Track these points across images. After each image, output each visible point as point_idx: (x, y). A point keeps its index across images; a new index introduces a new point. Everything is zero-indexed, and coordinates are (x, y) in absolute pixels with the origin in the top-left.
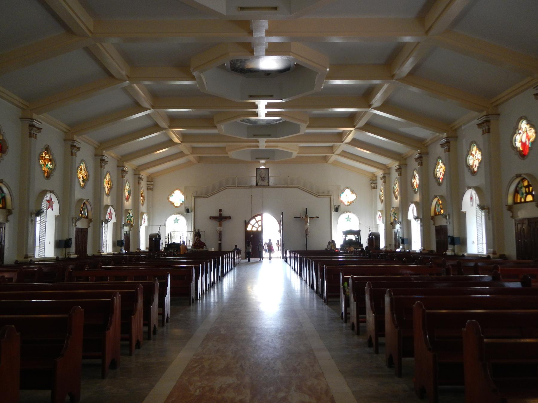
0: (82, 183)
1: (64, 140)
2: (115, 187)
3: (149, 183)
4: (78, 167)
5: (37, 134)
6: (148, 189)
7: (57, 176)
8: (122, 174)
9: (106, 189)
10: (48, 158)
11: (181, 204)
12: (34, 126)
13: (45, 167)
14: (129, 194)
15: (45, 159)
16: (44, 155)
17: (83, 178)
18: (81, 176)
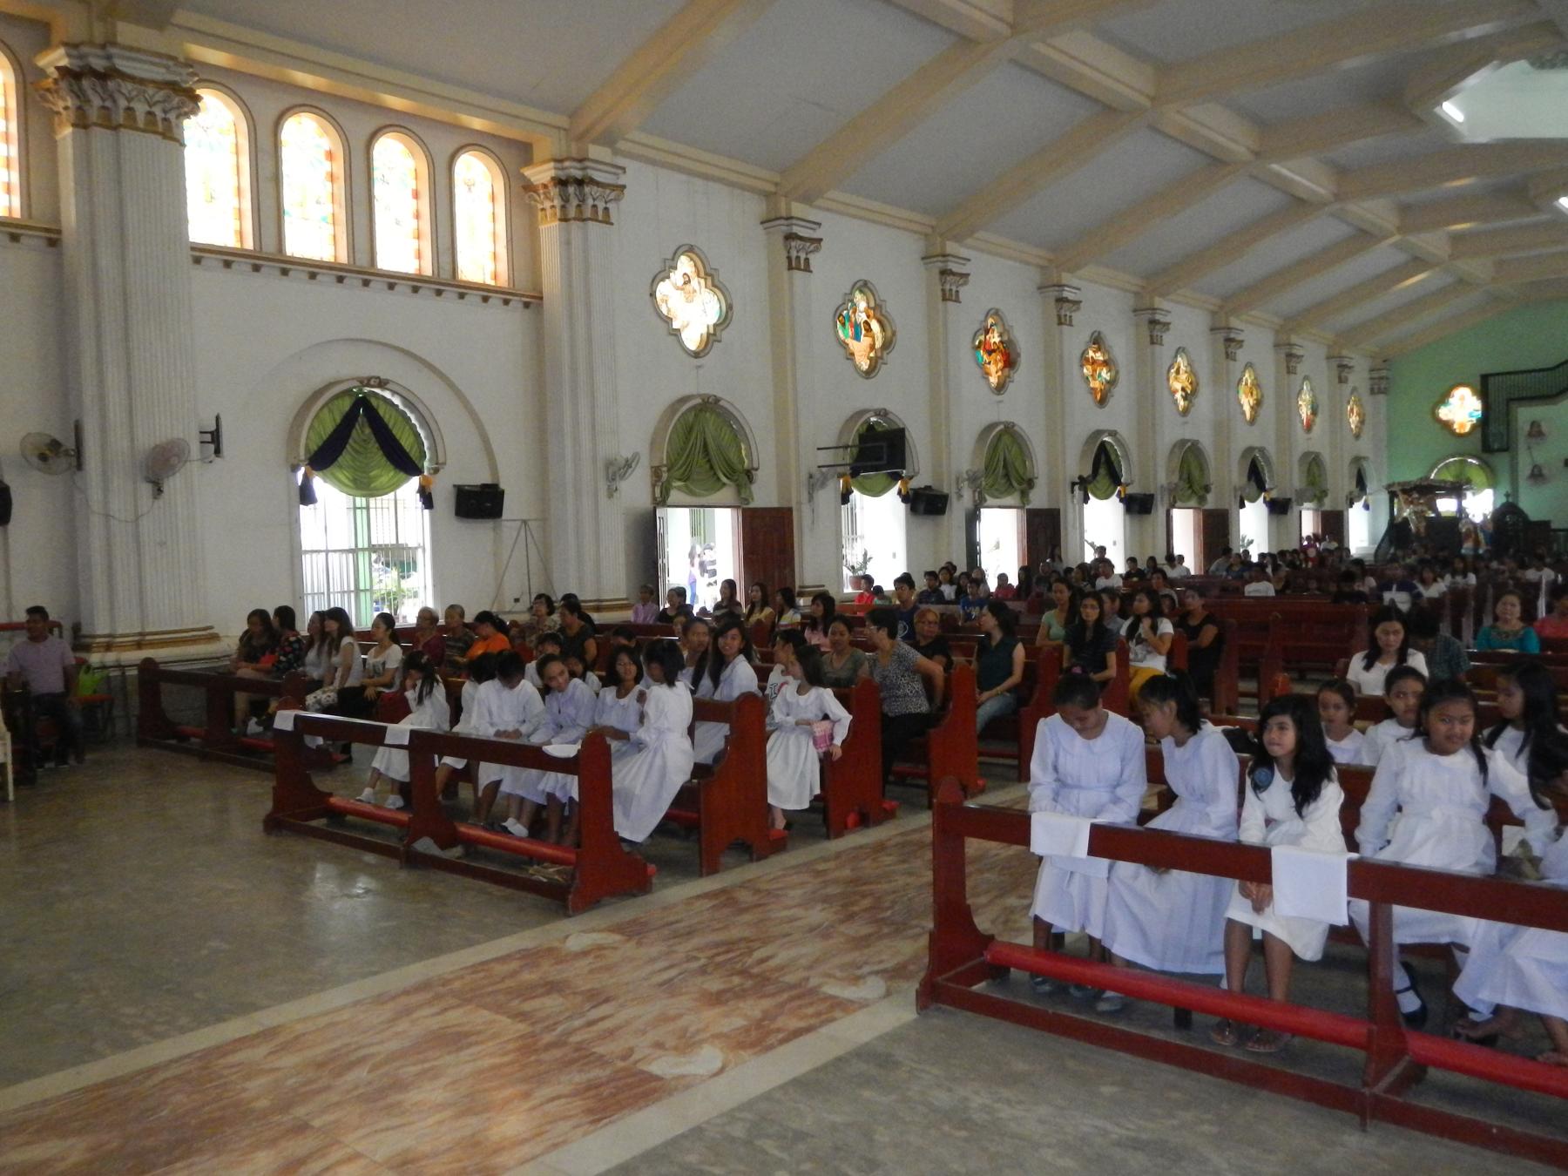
0: (1181, 403)
1: (1135, 311)
2: (1270, 402)
3: (1375, 375)
4: (1171, 367)
5: (1073, 314)
6: (1372, 392)
7: (1122, 396)
9: (1247, 408)
10: (1101, 358)
11: (1474, 427)
12: (1066, 300)
13: (1094, 379)
14: (1314, 412)
15: (1094, 362)
16: (1091, 354)
17: (1183, 389)
18: (1177, 386)
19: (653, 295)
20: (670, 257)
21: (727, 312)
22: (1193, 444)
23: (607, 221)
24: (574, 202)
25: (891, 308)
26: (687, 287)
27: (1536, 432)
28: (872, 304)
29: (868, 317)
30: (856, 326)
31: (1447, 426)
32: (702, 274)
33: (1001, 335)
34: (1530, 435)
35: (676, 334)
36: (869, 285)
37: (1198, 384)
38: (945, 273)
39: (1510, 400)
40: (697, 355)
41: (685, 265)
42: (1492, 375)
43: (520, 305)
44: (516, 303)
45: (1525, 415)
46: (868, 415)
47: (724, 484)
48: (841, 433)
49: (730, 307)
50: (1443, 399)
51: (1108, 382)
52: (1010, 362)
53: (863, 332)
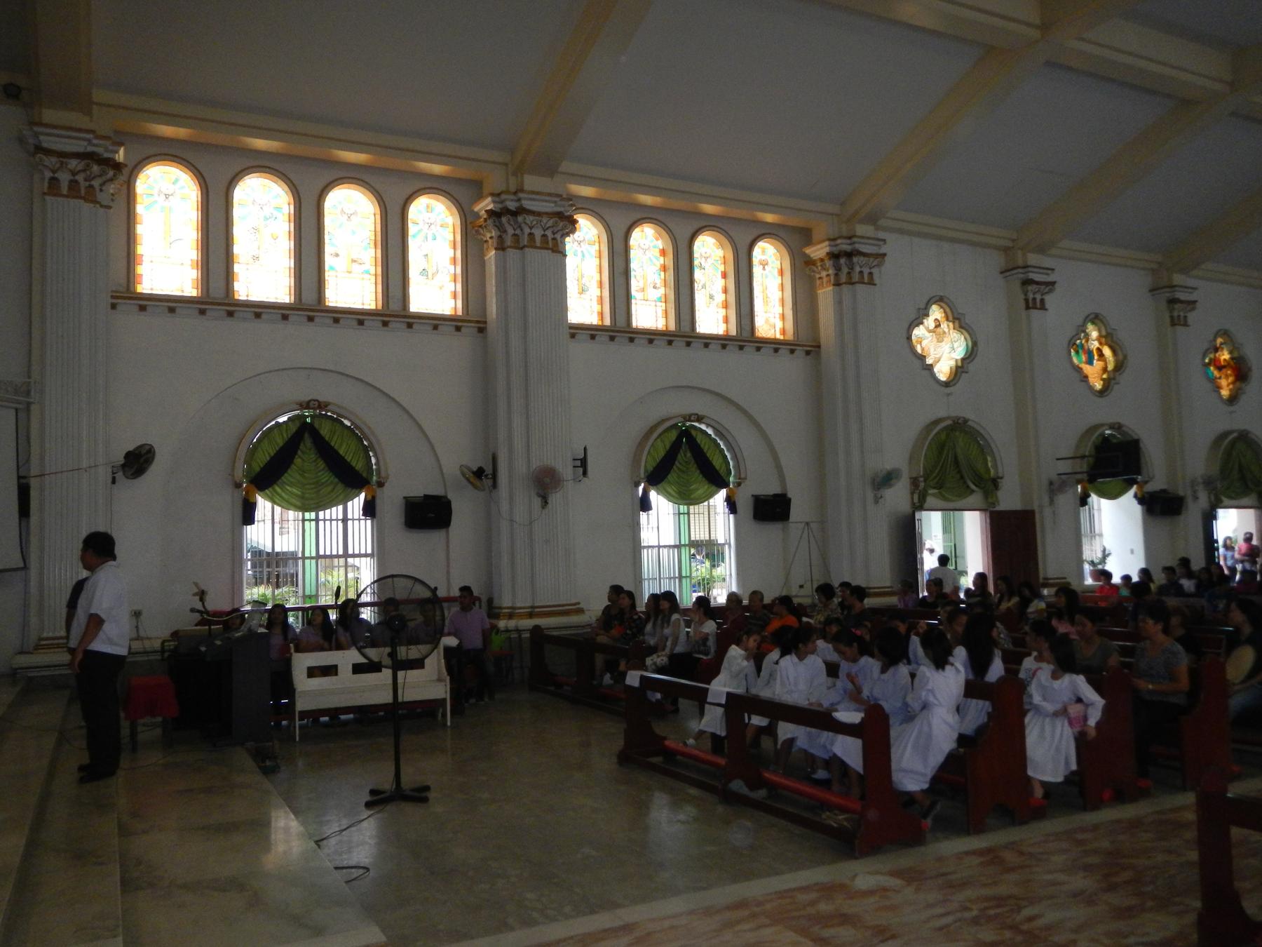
19: (909, 338)
20: (922, 306)
21: (973, 348)
24: (845, 270)
26: (938, 330)
28: (1104, 333)
29: (1101, 344)
30: (1090, 354)
32: (951, 318)
33: (1231, 352)
35: (930, 368)
38: (1172, 301)
40: (947, 384)
41: (936, 313)
43: (803, 354)
44: (800, 352)
46: (1104, 428)
47: (973, 491)
48: (1078, 447)
49: (975, 344)
53: (1096, 357)
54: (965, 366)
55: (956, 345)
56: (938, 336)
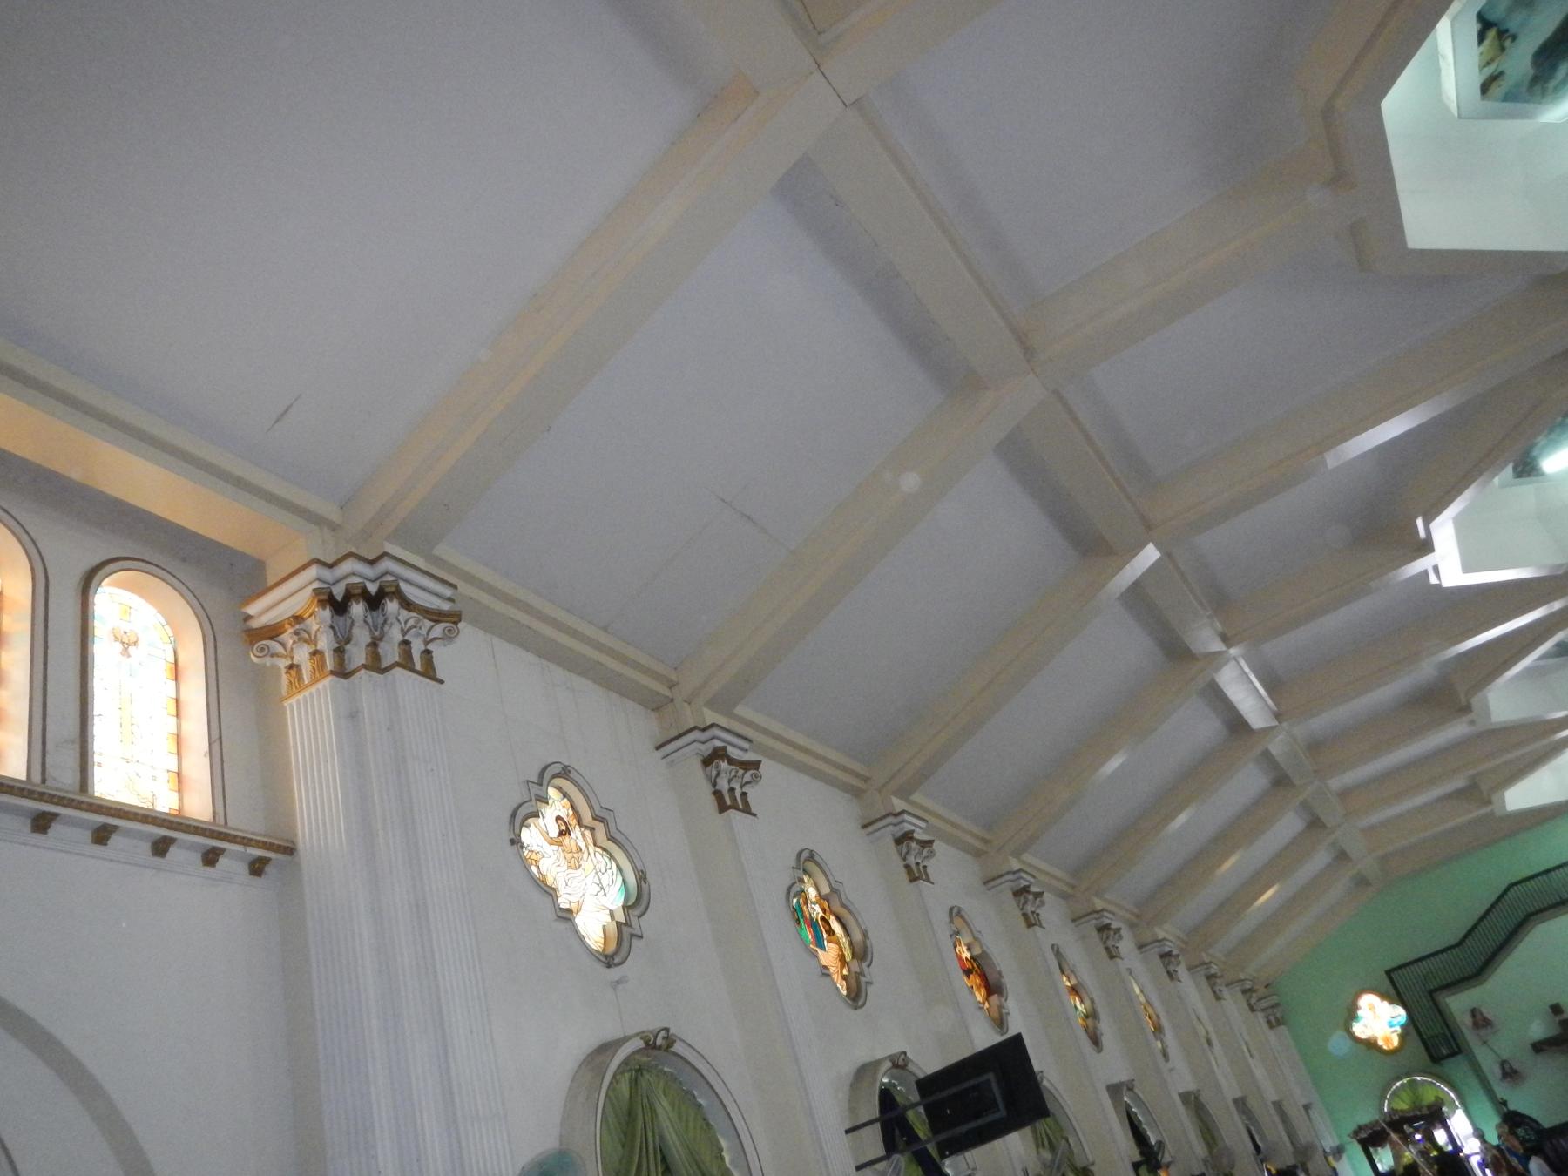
1: (1074, 920)
6: (1271, 1026)
8: (1212, 988)
11: (1403, 1037)
19: (516, 842)
20: (535, 779)
21: (639, 888)
22: (1196, 1098)
23: (429, 672)
24: (362, 636)
25: (850, 893)
26: (566, 840)
27: (1481, 1021)
28: (826, 890)
29: (824, 911)
30: (812, 924)
31: (1371, 1044)
32: (587, 818)
33: (969, 949)
34: (1476, 1025)
35: (567, 916)
36: (817, 858)
37: (1158, 1017)
38: (903, 839)
39: (1431, 993)
41: (556, 807)
42: (1395, 969)
43: (242, 869)
44: (233, 863)
45: (1458, 1004)
48: (852, 1110)
49: (642, 877)
50: (1352, 1014)
51: (1087, 1016)
52: (993, 988)
53: (825, 935)
54: (634, 921)
55: (606, 880)
56: (569, 856)
